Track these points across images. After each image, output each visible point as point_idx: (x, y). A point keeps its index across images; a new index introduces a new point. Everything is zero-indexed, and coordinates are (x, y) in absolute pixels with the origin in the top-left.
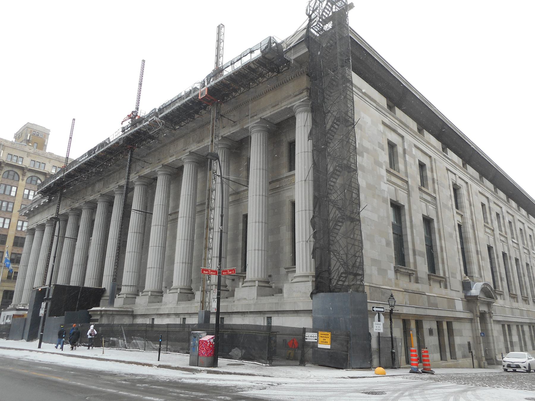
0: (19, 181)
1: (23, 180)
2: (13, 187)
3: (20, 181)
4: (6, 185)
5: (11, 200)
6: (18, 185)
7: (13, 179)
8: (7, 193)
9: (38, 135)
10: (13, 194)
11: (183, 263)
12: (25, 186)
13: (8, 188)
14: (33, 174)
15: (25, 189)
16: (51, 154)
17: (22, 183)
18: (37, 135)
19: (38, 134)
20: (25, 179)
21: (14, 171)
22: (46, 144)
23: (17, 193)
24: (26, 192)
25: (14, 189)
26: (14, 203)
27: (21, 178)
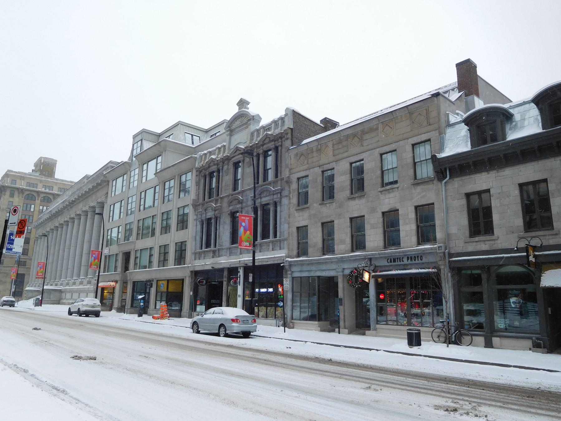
0: (35, 200)
1: (38, 200)
2: (32, 205)
3: (36, 200)
4: (27, 204)
5: (31, 214)
6: (35, 203)
7: (32, 200)
8: (28, 209)
9: (49, 165)
10: (32, 210)
11: (77, 267)
12: (40, 204)
13: (29, 206)
14: (45, 195)
15: (40, 206)
16: (57, 179)
17: (38, 202)
18: (48, 165)
19: (48, 164)
20: (40, 199)
21: (32, 194)
22: (54, 171)
23: (35, 209)
24: (41, 208)
25: (33, 206)
26: (33, 216)
27: (37, 198)
